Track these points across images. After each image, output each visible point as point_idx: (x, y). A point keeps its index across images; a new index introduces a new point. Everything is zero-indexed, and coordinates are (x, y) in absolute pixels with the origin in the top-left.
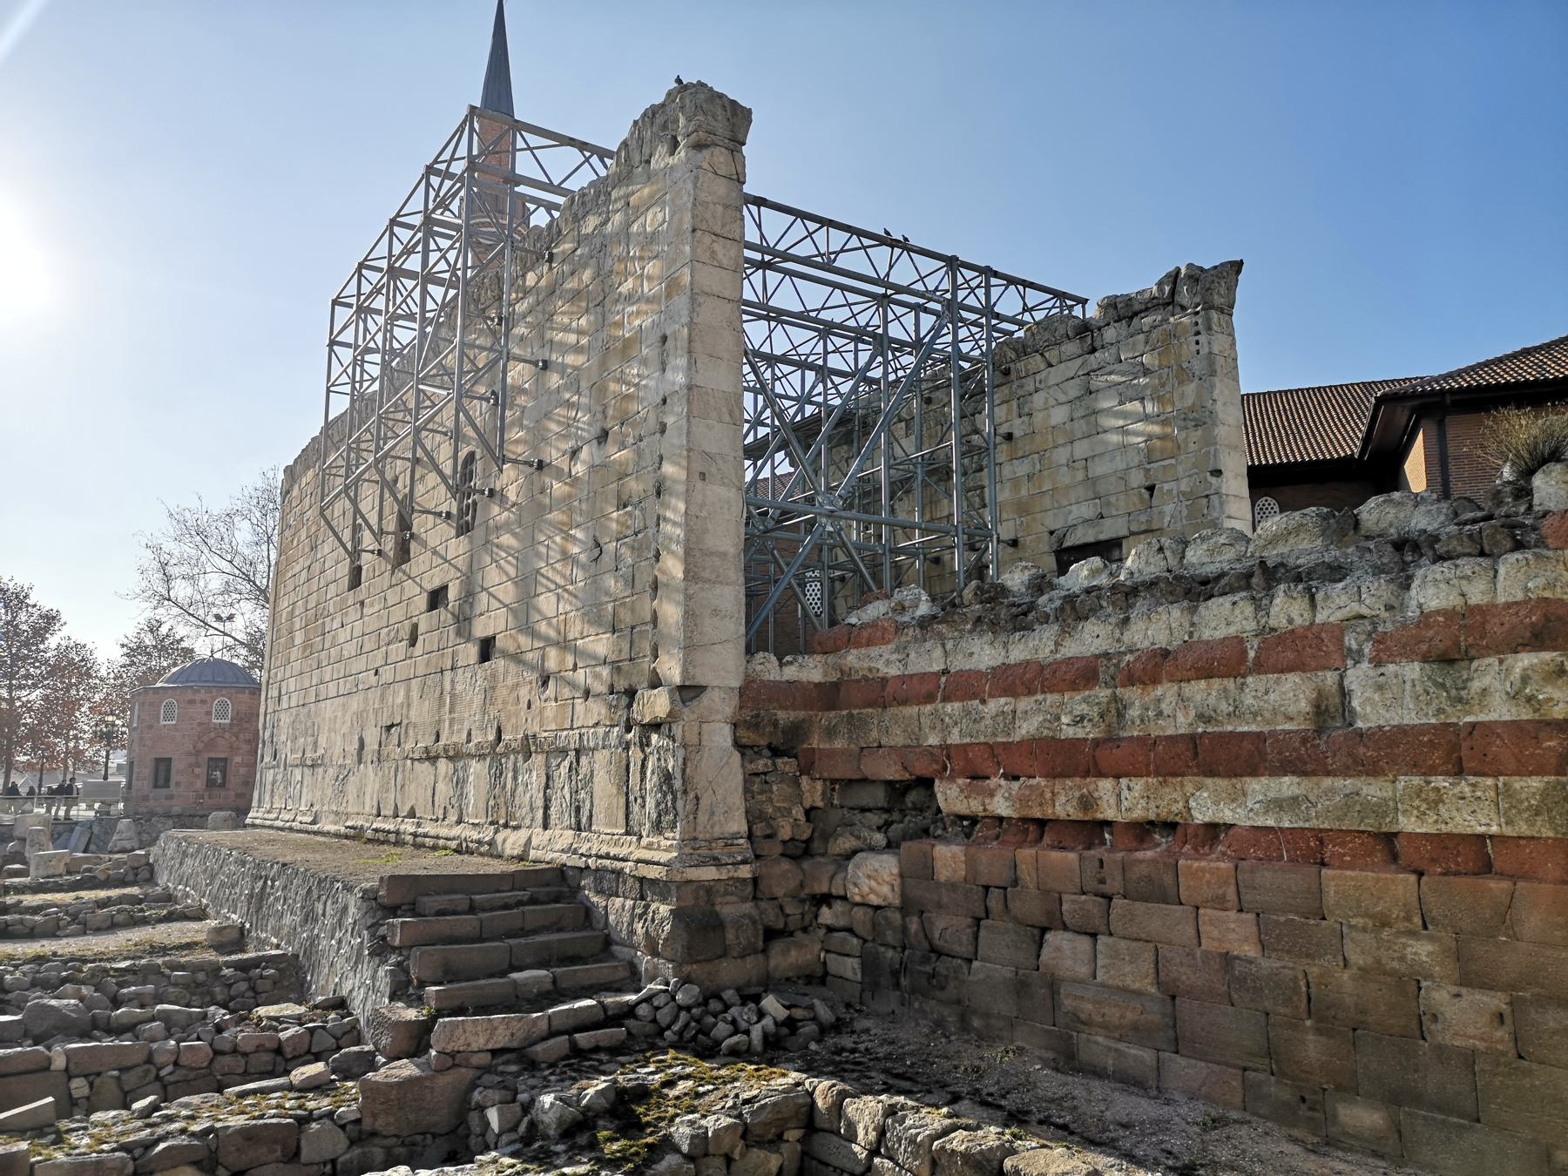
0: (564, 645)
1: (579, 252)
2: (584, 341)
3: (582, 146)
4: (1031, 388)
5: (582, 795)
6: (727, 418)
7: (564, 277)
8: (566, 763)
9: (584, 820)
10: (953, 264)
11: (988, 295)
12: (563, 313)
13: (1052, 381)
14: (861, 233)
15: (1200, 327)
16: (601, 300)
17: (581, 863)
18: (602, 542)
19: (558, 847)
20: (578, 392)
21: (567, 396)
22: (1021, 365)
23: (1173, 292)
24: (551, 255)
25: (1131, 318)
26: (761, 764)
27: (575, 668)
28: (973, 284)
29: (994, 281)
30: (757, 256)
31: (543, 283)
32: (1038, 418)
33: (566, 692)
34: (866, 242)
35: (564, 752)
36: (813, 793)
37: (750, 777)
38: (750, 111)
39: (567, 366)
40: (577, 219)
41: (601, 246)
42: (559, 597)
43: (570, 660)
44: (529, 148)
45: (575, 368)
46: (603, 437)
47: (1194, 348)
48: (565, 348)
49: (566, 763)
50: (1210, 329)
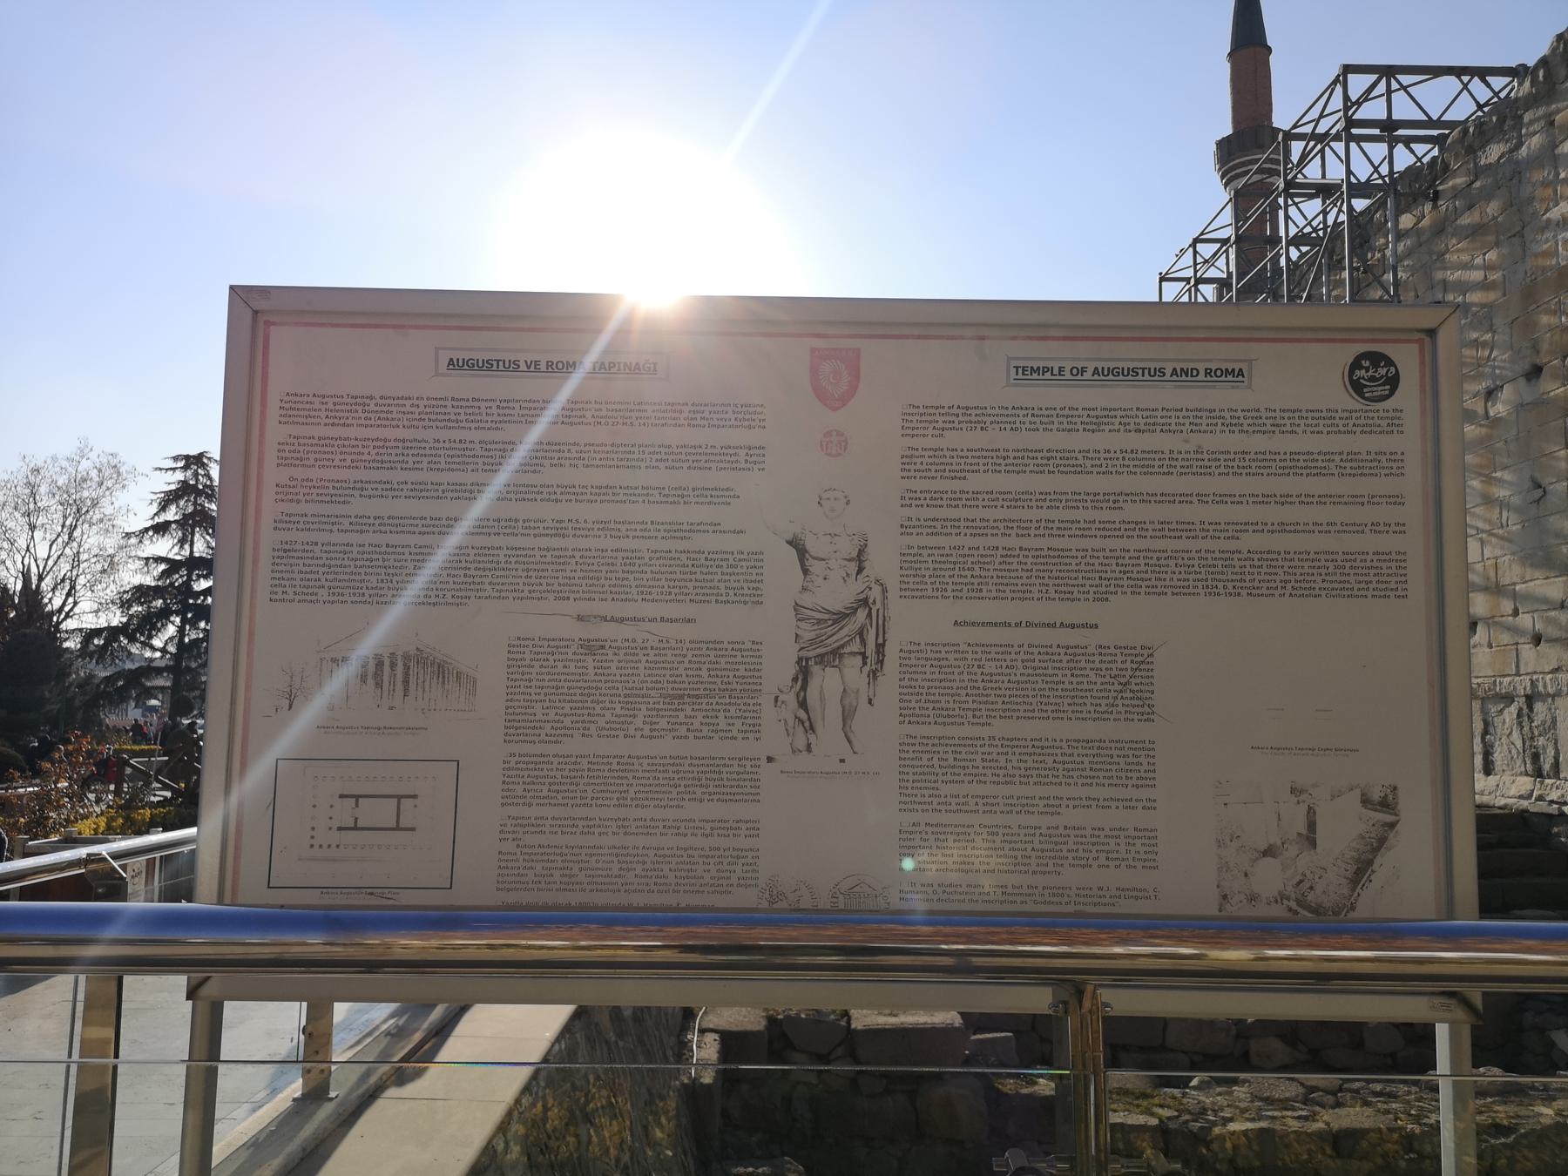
0: (1496, 590)
1: (1477, 184)
2: (1495, 276)
3: (1457, 71)
5: (1541, 741)
7: (1457, 213)
8: (1513, 709)
9: (1547, 767)
12: (1458, 251)
16: (1519, 227)
17: (1554, 809)
18: (1543, 484)
19: (1513, 792)
20: (1491, 329)
21: (1474, 335)
24: (1436, 193)
27: (1516, 613)
31: (1425, 222)
33: (1506, 638)
35: (1509, 699)
39: (1473, 304)
40: (1471, 151)
41: (1513, 173)
42: (1482, 542)
43: (1507, 606)
44: (1405, 88)
45: (1483, 306)
46: (1535, 372)
48: (1464, 287)
49: (1513, 709)
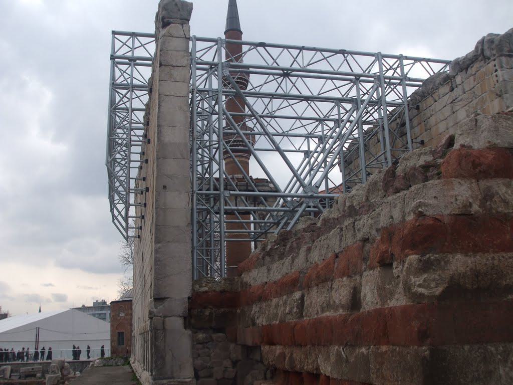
4: (429, 115)
6: (179, 156)
10: (379, 57)
11: (402, 70)
13: (437, 110)
14: (321, 50)
15: (497, 67)
22: (423, 103)
23: (483, 50)
25: (467, 69)
26: (201, 336)
28: (395, 66)
29: (405, 62)
30: (281, 72)
32: (434, 129)
34: (326, 54)
36: (235, 352)
37: (195, 343)
38: (192, 4)
47: (495, 79)
50: (502, 67)
